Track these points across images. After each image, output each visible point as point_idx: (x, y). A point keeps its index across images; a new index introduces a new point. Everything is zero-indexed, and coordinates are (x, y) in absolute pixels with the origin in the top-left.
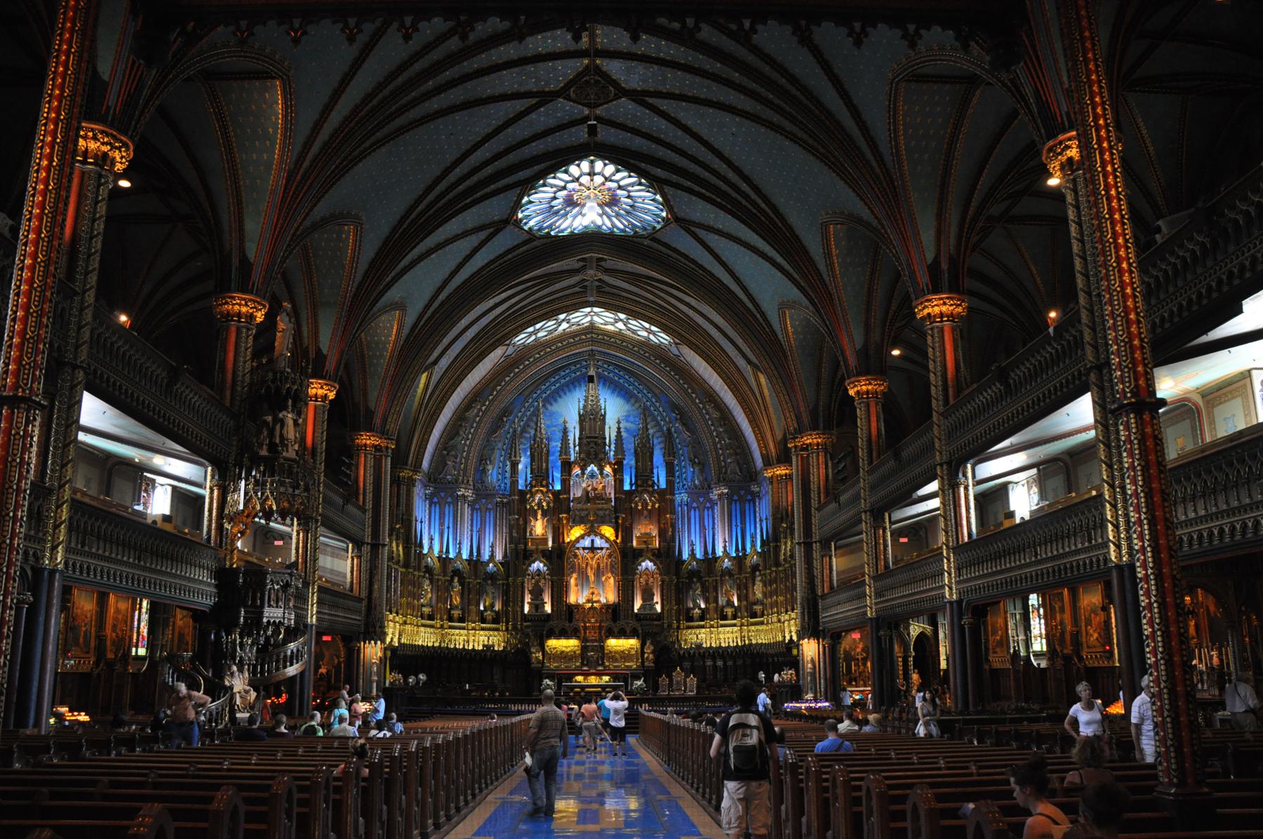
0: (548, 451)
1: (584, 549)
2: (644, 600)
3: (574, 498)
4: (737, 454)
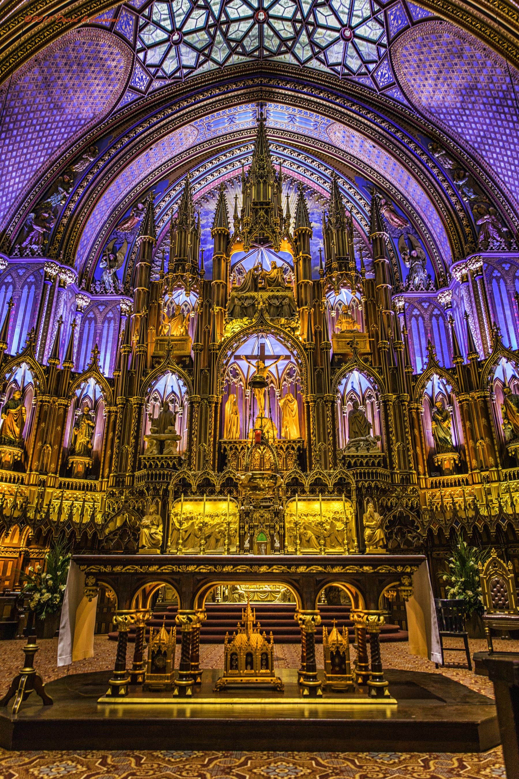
0: (196, 231)
1: (247, 357)
2: (353, 434)
3: (234, 289)
4: (489, 213)
